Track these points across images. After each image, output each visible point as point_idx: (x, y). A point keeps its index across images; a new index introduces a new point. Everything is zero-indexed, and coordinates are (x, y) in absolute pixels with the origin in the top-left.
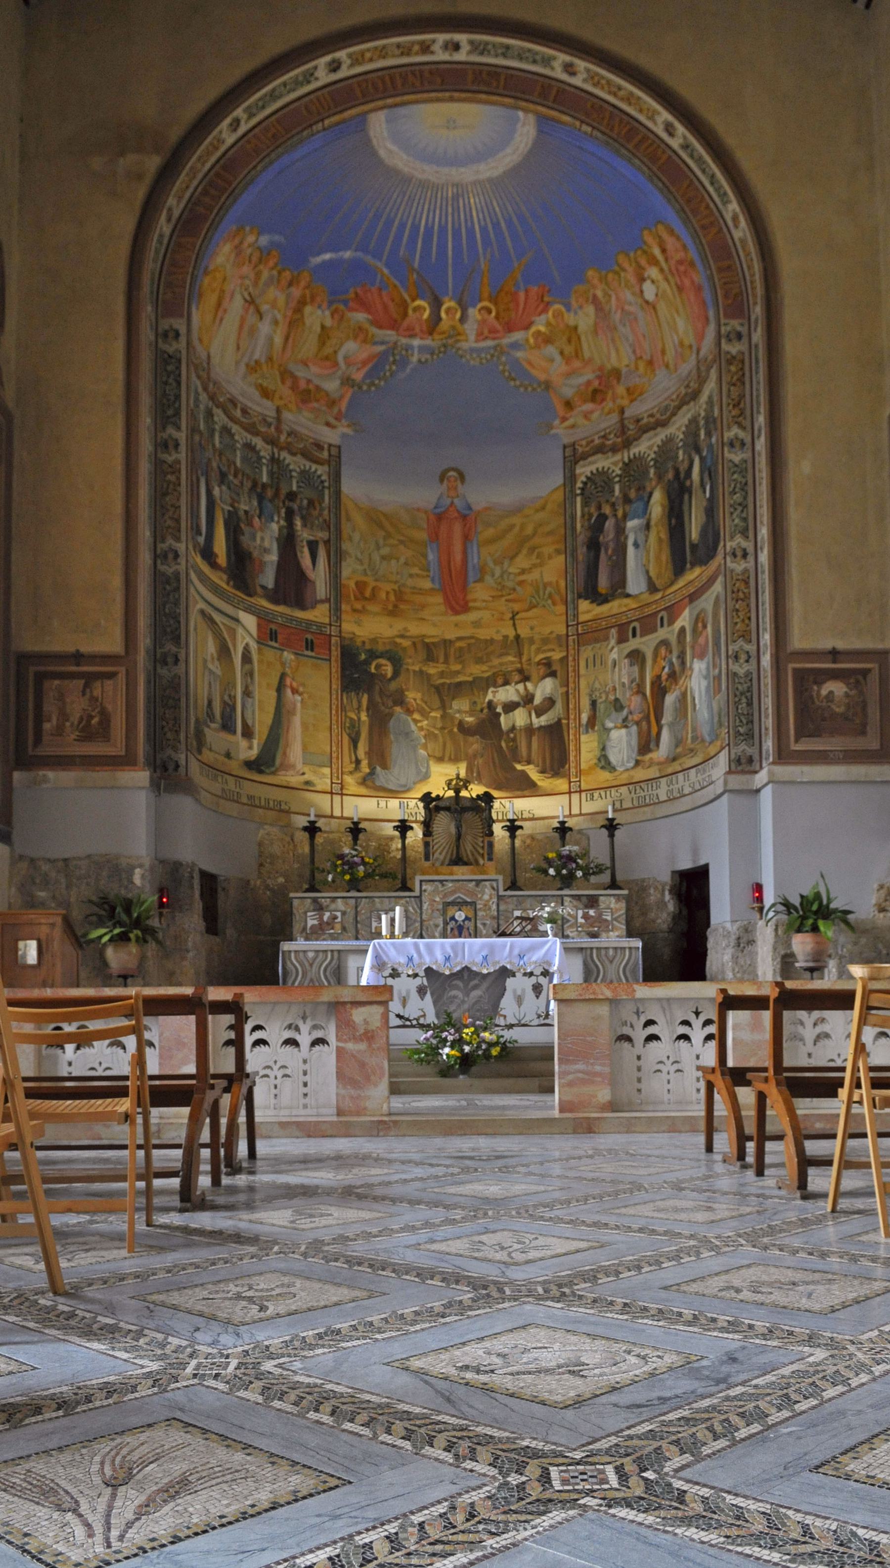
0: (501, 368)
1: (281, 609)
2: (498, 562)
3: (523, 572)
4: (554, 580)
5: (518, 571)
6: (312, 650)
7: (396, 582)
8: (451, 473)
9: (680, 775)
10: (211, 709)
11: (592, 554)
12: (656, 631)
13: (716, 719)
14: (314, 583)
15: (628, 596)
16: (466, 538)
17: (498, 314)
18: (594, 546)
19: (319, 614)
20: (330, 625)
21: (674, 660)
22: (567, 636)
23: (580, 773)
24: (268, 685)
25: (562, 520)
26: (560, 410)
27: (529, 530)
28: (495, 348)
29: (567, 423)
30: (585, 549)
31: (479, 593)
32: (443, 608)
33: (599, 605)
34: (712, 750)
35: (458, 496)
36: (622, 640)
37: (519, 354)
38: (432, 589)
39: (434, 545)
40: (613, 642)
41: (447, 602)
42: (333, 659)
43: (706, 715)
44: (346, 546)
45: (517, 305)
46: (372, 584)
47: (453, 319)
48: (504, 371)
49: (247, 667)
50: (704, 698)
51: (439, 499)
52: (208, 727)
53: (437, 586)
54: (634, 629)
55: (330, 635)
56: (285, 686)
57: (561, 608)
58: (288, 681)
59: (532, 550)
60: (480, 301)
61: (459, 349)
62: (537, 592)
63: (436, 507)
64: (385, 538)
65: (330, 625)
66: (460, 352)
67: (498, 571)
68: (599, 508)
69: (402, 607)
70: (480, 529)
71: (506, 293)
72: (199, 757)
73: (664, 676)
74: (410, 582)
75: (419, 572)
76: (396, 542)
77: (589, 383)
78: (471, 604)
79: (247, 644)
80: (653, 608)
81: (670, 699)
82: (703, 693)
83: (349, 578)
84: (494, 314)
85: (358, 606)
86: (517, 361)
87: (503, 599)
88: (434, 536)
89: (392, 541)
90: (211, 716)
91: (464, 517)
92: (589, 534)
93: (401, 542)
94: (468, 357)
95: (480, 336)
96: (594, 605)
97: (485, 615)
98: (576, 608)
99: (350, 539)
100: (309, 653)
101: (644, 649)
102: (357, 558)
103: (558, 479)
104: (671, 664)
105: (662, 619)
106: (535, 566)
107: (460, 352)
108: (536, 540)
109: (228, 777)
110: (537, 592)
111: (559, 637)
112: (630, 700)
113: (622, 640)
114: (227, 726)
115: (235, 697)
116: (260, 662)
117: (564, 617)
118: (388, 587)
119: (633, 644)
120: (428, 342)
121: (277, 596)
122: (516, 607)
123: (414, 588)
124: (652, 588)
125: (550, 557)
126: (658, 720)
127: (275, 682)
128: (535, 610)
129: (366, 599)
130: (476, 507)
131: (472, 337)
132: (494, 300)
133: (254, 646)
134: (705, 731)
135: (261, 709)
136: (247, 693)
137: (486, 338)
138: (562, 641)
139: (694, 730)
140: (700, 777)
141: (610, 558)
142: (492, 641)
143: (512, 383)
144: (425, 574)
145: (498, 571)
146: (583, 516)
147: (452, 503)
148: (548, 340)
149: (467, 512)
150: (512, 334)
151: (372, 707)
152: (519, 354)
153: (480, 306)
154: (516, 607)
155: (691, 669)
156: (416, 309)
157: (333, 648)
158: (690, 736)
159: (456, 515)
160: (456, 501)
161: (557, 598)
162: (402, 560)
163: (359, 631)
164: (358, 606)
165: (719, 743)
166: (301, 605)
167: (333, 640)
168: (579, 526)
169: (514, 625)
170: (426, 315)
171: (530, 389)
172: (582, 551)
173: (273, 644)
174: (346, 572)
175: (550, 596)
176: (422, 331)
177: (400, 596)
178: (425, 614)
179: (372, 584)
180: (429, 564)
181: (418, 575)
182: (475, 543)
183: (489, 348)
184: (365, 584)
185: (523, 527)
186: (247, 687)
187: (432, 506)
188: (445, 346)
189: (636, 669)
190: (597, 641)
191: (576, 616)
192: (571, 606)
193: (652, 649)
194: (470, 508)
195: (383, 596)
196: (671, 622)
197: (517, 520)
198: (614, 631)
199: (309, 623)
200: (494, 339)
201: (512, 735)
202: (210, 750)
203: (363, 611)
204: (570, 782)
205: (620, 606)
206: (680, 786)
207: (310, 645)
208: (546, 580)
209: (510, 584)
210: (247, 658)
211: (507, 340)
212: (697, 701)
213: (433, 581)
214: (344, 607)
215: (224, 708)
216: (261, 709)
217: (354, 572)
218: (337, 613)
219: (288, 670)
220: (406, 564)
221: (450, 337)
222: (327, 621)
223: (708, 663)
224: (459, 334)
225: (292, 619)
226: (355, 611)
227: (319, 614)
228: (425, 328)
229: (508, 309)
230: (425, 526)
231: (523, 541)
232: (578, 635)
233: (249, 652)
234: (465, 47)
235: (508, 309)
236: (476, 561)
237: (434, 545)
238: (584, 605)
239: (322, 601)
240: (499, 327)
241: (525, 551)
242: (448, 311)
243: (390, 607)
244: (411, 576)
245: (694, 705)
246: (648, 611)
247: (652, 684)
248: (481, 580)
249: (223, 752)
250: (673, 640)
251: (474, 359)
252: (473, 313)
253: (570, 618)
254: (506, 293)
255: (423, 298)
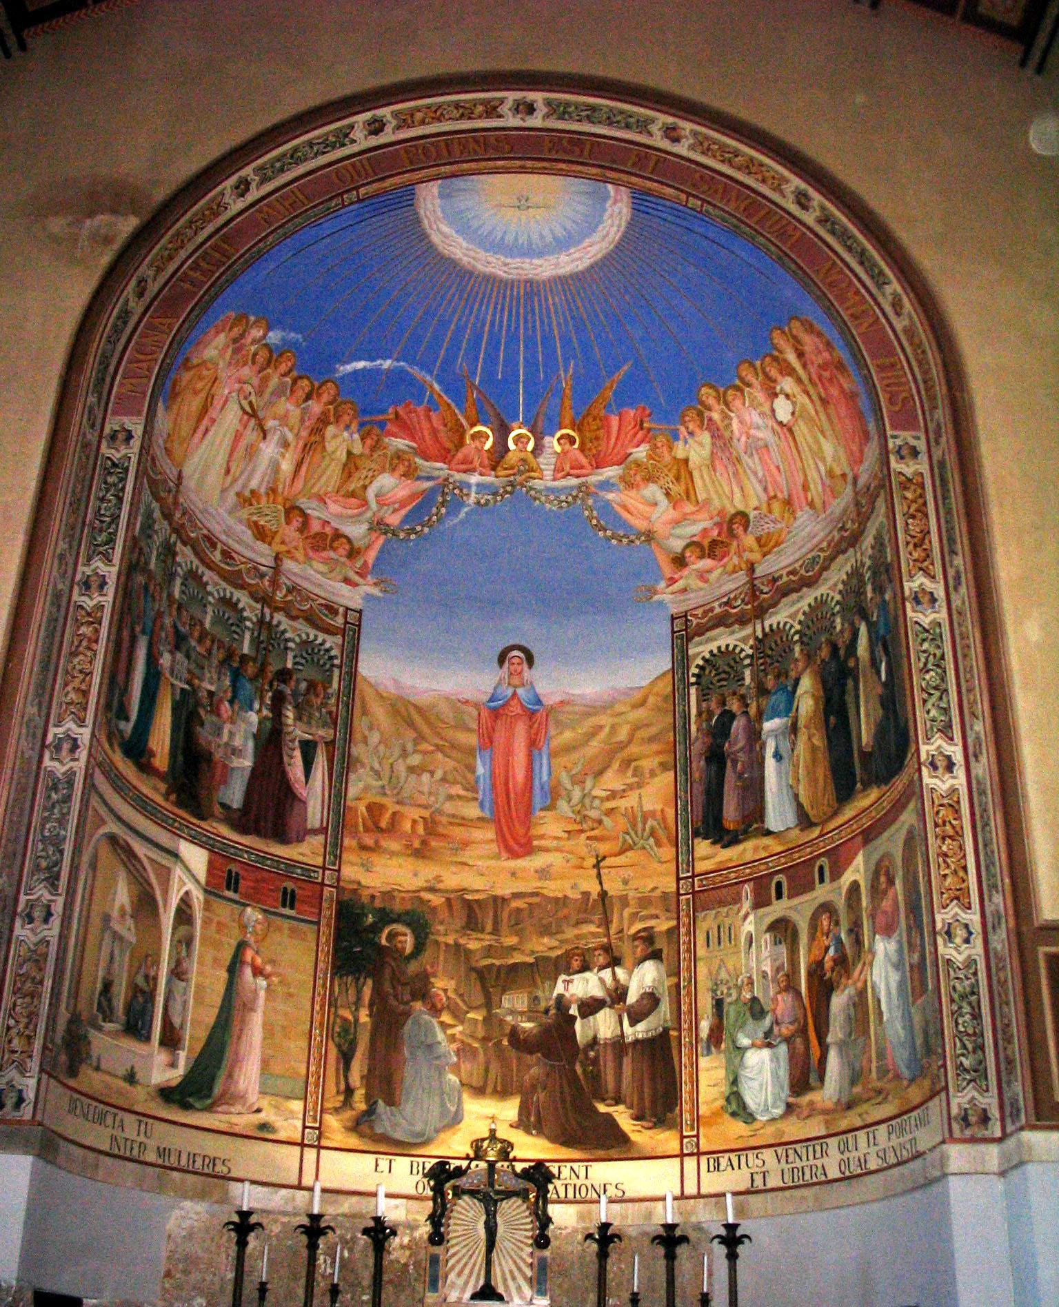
0: (587, 513)
1: (246, 840)
2: (578, 781)
3: (613, 795)
4: (659, 807)
5: (604, 794)
6: (292, 907)
7: (426, 807)
8: (515, 653)
9: (862, 1135)
10: (109, 1000)
11: (714, 768)
12: (813, 889)
13: (919, 1041)
14: (305, 803)
15: (768, 833)
16: (533, 744)
17: (582, 444)
18: (716, 758)
19: (308, 851)
20: (324, 868)
21: (843, 936)
22: (678, 894)
23: (697, 1120)
24: (215, 960)
25: (669, 719)
26: (667, 570)
27: (623, 734)
28: (579, 487)
29: (680, 585)
30: (703, 763)
31: (550, 826)
32: (494, 847)
33: (724, 847)
34: (915, 1094)
35: (523, 685)
36: (760, 902)
37: (610, 496)
38: (479, 819)
39: (487, 755)
40: (746, 905)
41: (502, 839)
42: (323, 922)
43: (902, 1033)
44: (358, 750)
45: (609, 433)
46: (392, 807)
47: (524, 450)
48: (590, 518)
49: (183, 930)
50: (895, 1001)
51: (495, 688)
52: (100, 1029)
53: (487, 814)
54: (779, 885)
55: (323, 884)
56: (243, 963)
57: (668, 852)
58: (249, 955)
59: (627, 763)
60: (561, 429)
61: (531, 488)
62: (634, 826)
63: (491, 700)
64: (416, 742)
65: (324, 868)
66: (533, 493)
67: (577, 794)
68: (723, 703)
69: (433, 844)
70: (552, 732)
71: (594, 419)
72: (72, 1082)
73: (828, 964)
74: (449, 807)
75: (462, 792)
76: (432, 748)
77: (705, 531)
78: (535, 843)
79: (187, 893)
80: (807, 854)
81: (838, 1002)
82: (894, 991)
83: (358, 799)
84: (576, 446)
85: (369, 840)
86: (608, 503)
87: (583, 836)
88: (488, 741)
89: (424, 746)
90: (107, 1013)
91: (531, 714)
92: (708, 740)
93: (439, 748)
94: (543, 499)
95: (559, 471)
96: (718, 846)
97: (555, 859)
98: (691, 851)
99: (365, 740)
100: (287, 911)
101: (794, 916)
102: (372, 769)
103: (662, 662)
104: (839, 941)
105: (821, 868)
106: (631, 787)
107: (533, 493)
108: (634, 749)
109: (121, 1114)
110: (634, 826)
111: (665, 896)
112: (775, 1000)
113: (760, 902)
114: (136, 1027)
115: (155, 979)
116: (207, 922)
117: (673, 866)
118: (416, 813)
119: (778, 909)
120: (490, 479)
121: (244, 821)
122: (603, 848)
123: (454, 816)
124: (805, 821)
125: (653, 774)
126: (821, 1036)
127: (227, 956)
128: (629, 854)
129: (382, 830)
130: (544, 700)
131: (548, 474)
132: (579, 428)
133: (198, 896)
134: (900, 1057)
135: (199, 999)
136: (178, 973)
137: (569, 474)
138: (670, 902)
139: (881, 1055)
140: (895, 1141)
141: (740, 776)
142: (562, 901)
143: (601, 534)
144: (470, 795)
145: (577, 794)
146: (699, 714)
147: (515, 694)
148: (649, 479)
149: (536, 707)
150: (600, 471)
151: (379, 996)
152: (610, 496)
153: (558, 435)
154: (603, 848)
155: (872, 952)
156: (473, 437)
157: (325, 905)
158: (874, 1065)
159: (519, 711)
160: (520, 691)
161: (661, 833)
162: (439, 774)
163: (366, 880)
164: (369, 840)
165: (927, 1083)
166: (281, 835)
167: (327, 890)
168: (694, 728)
169: (599, 876)
170: (488, 445)
171: (625, 541)
172: (699, 765)
173: (230, 894)
174: (352, 792)
175: (653, 833)
176: (481, 465)
177: (431, 826)
178: (465, 856)
179: (392, 807)
180: (477, 781)
181: (459, 797)
182: (545, 750)
183: (572, 488)
184: (382, 807)
185: (614, 728)
186: (179, 963)
187: (485, 698)
188: (512, 484)
189: (783, 950)
190: (722, 903)
191: (691, 863)
192: (684, 849)
193: (809, 914)
194: (539, 702)
195: (407, 826)
196: (836, 874)
197: (605, 720)
198: (747, 888)
199: (292, 864)
200: (578, 477)
201: (592, 1054)
202: (97, 1069)
203: (376, 849)
204: (682, 1137)
205: (756, 849)
206: (860, 1154)
207: (289, 899)
208: (647, 807)
209: (593, 814)
210: (184, 915)
211: (593, 479)
212: (884, 1007)
213: (482, 806)
214: (347, 842)
215: (135, 997)
216: (199, 999)
217: (366, 789)
218: (335, 851)
219: (250, 938)
220: (444, 780)
221: (520, 473)
222: (319, 861)
223: (900, 942)
224: (532, 470)
225: (264, 857)
226: (364, 848)
227: (308, 851)
228: (486, 462)
229: (597, 438)
230: (474, 726)
231: (613, 750)
232: (694, 893)
233: (190, 907)
234: (541, 110)
235: (597, 438)
236: (545, 778)
237: (487, 755)
238: (703, 847)
239: (315, 832)
240: (584, 461)
241: (616, 765)
242: (518, 439)
243: (417, 844)
244: (450, 798)
245: (881, 1014)
246: (798, 858)
247: (810, 974)
248: (551, 807)
249: (122, 1071)
250: (841, 903)
251: (551, 502)
252: (553, 444)
253: (683, 866)
254: (594, 419)
255: (485, 424)
